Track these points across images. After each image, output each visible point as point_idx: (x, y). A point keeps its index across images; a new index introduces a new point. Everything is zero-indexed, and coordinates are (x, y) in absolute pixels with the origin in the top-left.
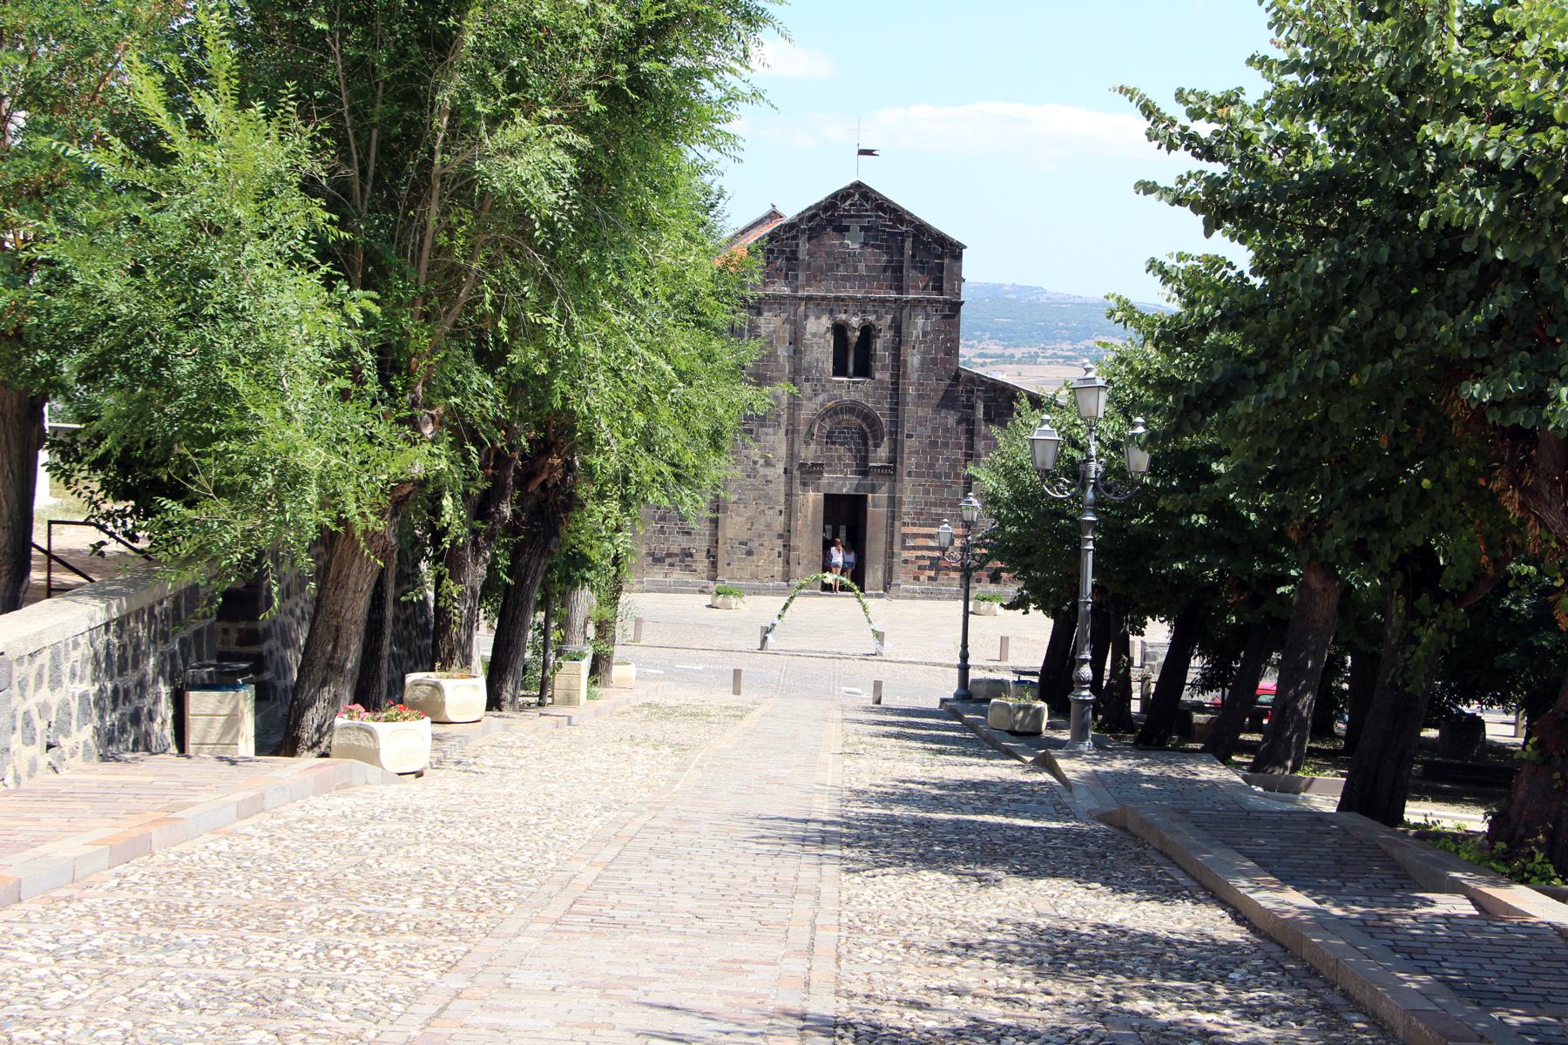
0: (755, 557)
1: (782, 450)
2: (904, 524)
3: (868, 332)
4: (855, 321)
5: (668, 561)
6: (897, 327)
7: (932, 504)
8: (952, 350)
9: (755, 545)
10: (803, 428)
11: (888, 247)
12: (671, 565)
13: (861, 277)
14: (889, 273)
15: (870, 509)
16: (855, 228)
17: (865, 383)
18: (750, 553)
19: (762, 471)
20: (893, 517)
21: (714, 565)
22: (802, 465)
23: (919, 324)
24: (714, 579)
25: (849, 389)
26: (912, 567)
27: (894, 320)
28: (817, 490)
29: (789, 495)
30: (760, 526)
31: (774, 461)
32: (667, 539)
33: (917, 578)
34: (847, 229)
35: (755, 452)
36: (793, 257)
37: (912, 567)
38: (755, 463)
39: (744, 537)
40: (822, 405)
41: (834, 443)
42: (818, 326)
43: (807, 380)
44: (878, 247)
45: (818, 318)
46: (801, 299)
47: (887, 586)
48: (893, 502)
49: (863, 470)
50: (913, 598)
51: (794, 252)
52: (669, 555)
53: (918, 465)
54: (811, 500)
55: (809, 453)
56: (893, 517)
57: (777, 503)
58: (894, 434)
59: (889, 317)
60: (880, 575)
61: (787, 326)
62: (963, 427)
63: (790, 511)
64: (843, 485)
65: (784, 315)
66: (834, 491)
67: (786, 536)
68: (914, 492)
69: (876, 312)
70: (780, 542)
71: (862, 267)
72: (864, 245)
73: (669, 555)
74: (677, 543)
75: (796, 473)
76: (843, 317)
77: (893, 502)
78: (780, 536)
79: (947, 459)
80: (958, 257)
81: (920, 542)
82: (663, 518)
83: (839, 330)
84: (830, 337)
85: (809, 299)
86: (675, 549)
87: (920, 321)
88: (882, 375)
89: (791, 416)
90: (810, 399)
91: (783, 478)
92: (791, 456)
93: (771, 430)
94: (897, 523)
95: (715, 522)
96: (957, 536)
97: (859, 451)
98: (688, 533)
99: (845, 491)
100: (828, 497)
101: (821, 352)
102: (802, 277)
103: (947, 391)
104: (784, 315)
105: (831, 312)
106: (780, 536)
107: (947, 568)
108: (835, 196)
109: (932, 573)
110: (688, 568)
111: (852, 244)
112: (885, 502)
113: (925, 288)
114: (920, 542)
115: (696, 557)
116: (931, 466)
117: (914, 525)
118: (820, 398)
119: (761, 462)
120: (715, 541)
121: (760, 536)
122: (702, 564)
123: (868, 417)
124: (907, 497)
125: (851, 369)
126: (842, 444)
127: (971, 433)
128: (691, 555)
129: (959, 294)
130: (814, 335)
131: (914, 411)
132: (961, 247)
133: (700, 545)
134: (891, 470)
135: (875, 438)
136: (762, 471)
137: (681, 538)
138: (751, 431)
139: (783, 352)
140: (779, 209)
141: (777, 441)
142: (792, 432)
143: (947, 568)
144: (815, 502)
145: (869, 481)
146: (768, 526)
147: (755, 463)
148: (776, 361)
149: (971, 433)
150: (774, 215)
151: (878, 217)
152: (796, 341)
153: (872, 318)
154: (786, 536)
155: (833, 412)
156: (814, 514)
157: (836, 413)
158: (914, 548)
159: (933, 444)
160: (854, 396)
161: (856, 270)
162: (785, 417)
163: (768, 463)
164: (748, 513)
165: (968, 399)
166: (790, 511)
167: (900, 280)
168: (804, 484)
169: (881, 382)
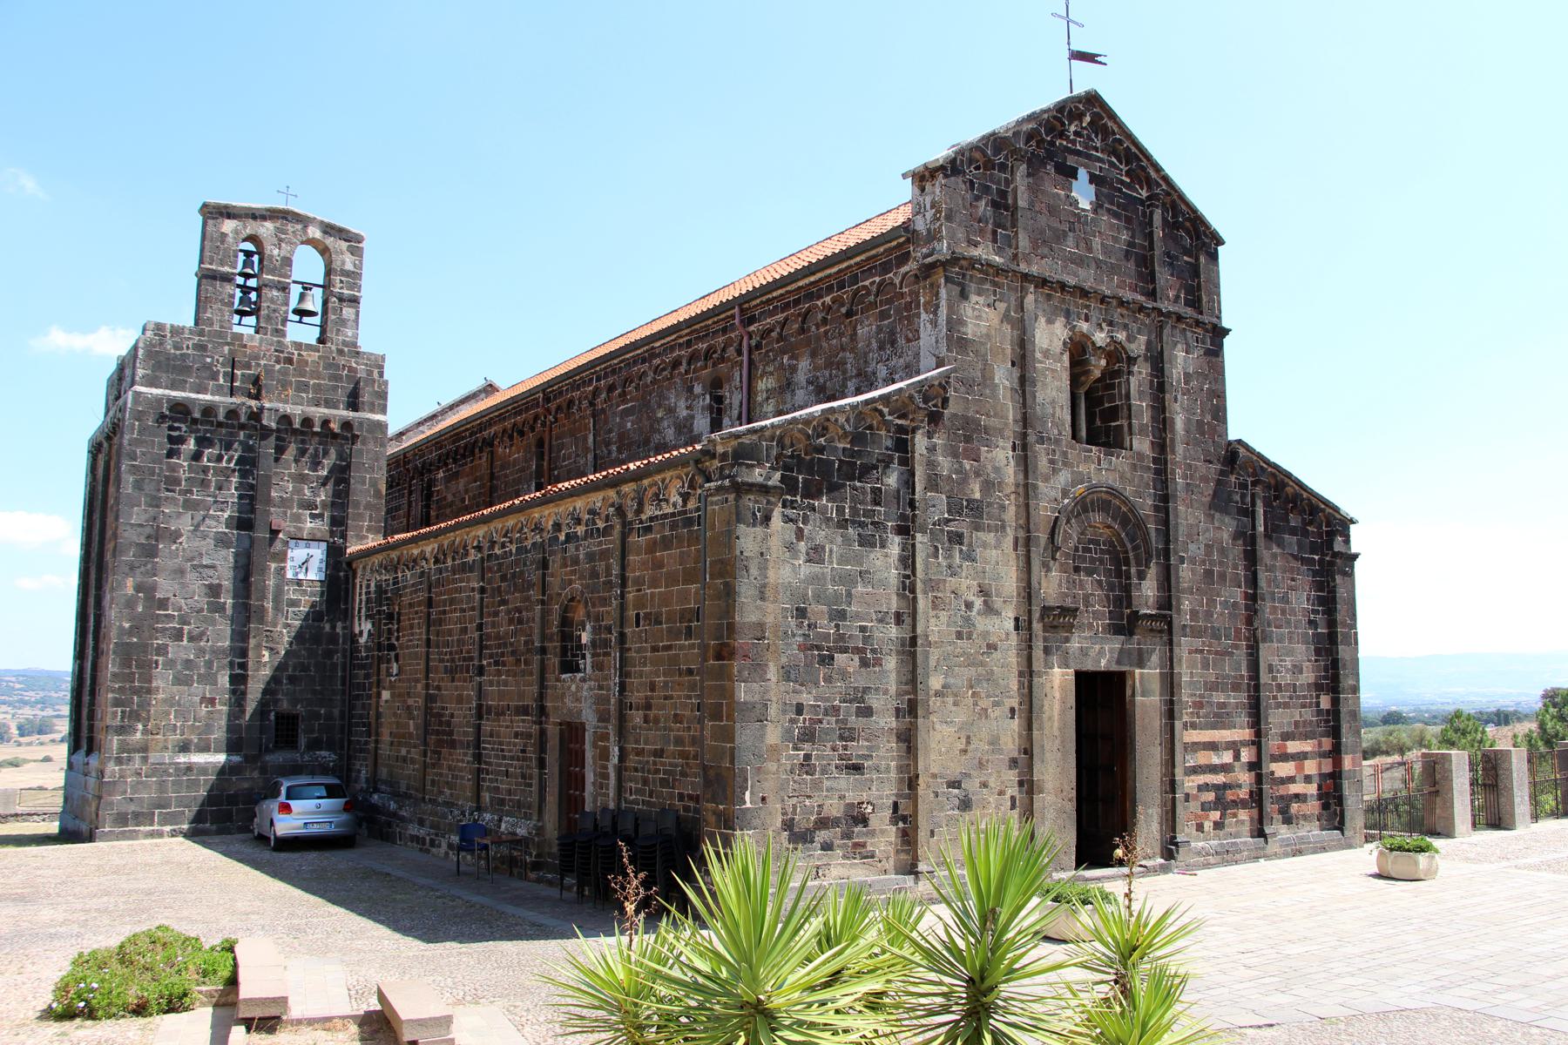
0: (976, 812)
1: (1010, 581)
2: (1185, 726)
3: (1118, 357)
4: (1100, 338)
5: (822, 836)
6: (1158, 362)
7: (1213, 687)
8: (1219, 413)
9: (971, 786)
10: (1042, 536)
11: (1128, 220)
12: (827, 847)
13: (1098, 263)
14: (1131, 265)
15: (1138, 698)
16: (1083, 174)
17: (1120, 461)
18: (965, 805)
19: (982, 624)
20: (1171, 714)
21: (908, 838)
22: (1046, 610)
23: (1182, 361)
24: (911, 869)
25: (1101, 470)
26: (1194, 806)
27: (1149, 343)
28: (1065, 664)
29: (1028, 673)
30: (980, 746)
31: (997, 602)
32: (817, 785)
33: (1200, 828)
34: (1073, 174)
35: (966, 584)
36: (1002, 203)
37: (1194, 806)
38: (969, 605)
39: (954, 771)
40: (1065, 493)
41: (1077, 570)
42: (1050, 336)
43: (1041, 440)
44: (1116, 215)
45: (1050, 322)
46: (1026, 277)
47: (1169, 849)
48: (1170, 683)
49: (1125, 623)
50: (1207, 866)
51: (1003, 194)
52: (823, 823)
53: (1194, 614)
54: (1058, 682)
55: (1052, 585)
56: (1171, 714)
57: (1005, 692)
58: (1166, 553)
59: (1143, 339)
60: (1155, 826)
61: (1007, 328)
62: (1239, 549)
63: (1029, 710)
64: (1101, 653)
65: (1002, 306)
66: (1089, 666)
67: (1026, 758)
68: (1192, 665)
69: (1126, 327)
70: (1012, 776)
71: (1096, 242)
72: (1097, 206)
73: (823, 823)
74: (838, 792)
75: (1037, 627)
76: (1084, 326)
77: (1170, 683)
78: (1014, 763)
79: (1225, 604)
80: (1214, 257)
81: (1203, 758)
82: (808, 736)
83: (1078, 351)
84: (1066, 357)
85: (1042, 282)
86: (834, 808)
87: (1180, 354)
88: (1142, 444)
89: (1026, 509)
90: (1047, 479)
91: (1014, 639)
92: (1028, 592)
93: (990, 537)
94: (1178, 724)
95: (908, 740)
96: (1244, 743)
97: (1111, 588)
98: (857, 768)
99: (1103, 665)
100: (1079, 675)
101: (1054, 391)
102: (1024, 242)
103: (1218, 483)
104: (1002, 306)
105: (1068, 315)
106: (1014, 763)
107: (1236, 804)
108: (1061, 107)
109: (1215, 815)
110: (859, 851)
111: (1083, 194)
112: (1156, 686)
113: (1177, 297)
114: (1203, 758)
115: (874, 822)
116: (1209, 614)
117: (1194, 726)
118: (1064, 477)
119: (978, 603)
120: (911, 782)
121: (981, 765)
122: (884, 838)
123: (1128, 519)
124: (1186, 673)
125: (1084, 433)
126: (1090, 573)
127: (1251, 558)
128: (864, 821)
129: (1219, 318)
130: (1046, 353)
131: (1189, 515)
132: (1220, 242)
133: (880, 792)
134: (1164, 623)
135: (1138, 564)
136: (982, 624)
137: (844, 781)
138: (957, 538)
139: (1003, 376)
140: (498, 383)
141: (998, 560)
142: (1025, 543)
143: (1236, 804)
144: (1063, 688)
145: (1133, 645)
146: (994, 742)
147: (969, 605)
148: (994, 396)
149: (1251, 558)
150: (490, 389)
151: (1112, 164)
152: (1022, 358)
153: (1121, 336)
154: (1026, 758)
155: (1084, 506)
156: (1063, 712)
157: (1086, 510)
158: (1195, 770)
159: (1209, 574)
160: (1112, 480)
161: (1090, 249)
162: (1011, 514)
163: (989, 610)
164: (960, 716)
165: (1243, 496)
166: (1029, 710)
167: (1152, 278)
168: (1047, 651)
169: (1140, 456)
